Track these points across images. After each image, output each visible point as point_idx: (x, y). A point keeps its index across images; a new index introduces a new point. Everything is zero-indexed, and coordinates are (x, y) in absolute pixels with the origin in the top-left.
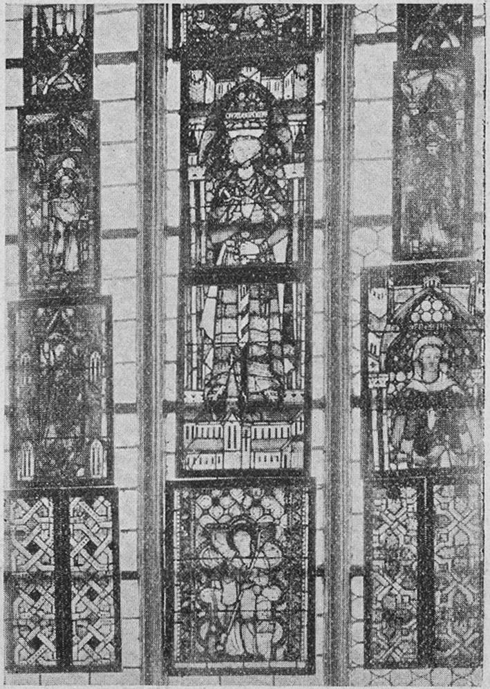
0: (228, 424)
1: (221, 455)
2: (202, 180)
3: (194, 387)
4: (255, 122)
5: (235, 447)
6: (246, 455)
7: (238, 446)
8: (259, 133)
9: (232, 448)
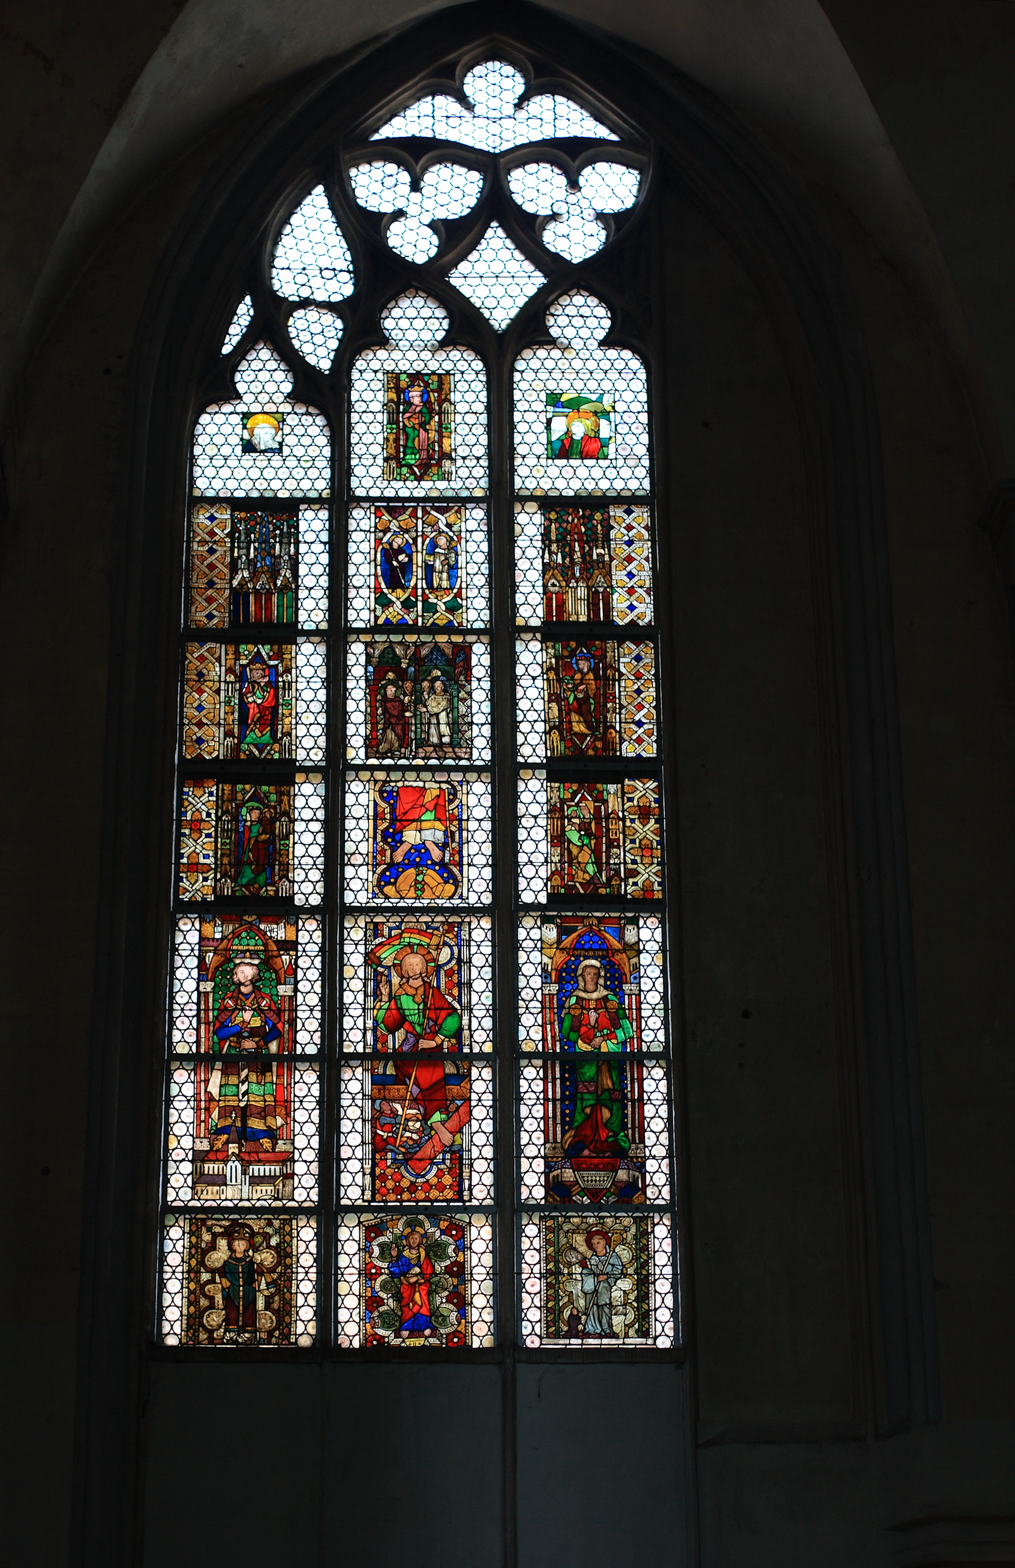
0: (230, 1163)
3: (202, 1135)
6: (246, 1188)
7: (239, 1181)
8: (256, 962)
9: (234, 1182)
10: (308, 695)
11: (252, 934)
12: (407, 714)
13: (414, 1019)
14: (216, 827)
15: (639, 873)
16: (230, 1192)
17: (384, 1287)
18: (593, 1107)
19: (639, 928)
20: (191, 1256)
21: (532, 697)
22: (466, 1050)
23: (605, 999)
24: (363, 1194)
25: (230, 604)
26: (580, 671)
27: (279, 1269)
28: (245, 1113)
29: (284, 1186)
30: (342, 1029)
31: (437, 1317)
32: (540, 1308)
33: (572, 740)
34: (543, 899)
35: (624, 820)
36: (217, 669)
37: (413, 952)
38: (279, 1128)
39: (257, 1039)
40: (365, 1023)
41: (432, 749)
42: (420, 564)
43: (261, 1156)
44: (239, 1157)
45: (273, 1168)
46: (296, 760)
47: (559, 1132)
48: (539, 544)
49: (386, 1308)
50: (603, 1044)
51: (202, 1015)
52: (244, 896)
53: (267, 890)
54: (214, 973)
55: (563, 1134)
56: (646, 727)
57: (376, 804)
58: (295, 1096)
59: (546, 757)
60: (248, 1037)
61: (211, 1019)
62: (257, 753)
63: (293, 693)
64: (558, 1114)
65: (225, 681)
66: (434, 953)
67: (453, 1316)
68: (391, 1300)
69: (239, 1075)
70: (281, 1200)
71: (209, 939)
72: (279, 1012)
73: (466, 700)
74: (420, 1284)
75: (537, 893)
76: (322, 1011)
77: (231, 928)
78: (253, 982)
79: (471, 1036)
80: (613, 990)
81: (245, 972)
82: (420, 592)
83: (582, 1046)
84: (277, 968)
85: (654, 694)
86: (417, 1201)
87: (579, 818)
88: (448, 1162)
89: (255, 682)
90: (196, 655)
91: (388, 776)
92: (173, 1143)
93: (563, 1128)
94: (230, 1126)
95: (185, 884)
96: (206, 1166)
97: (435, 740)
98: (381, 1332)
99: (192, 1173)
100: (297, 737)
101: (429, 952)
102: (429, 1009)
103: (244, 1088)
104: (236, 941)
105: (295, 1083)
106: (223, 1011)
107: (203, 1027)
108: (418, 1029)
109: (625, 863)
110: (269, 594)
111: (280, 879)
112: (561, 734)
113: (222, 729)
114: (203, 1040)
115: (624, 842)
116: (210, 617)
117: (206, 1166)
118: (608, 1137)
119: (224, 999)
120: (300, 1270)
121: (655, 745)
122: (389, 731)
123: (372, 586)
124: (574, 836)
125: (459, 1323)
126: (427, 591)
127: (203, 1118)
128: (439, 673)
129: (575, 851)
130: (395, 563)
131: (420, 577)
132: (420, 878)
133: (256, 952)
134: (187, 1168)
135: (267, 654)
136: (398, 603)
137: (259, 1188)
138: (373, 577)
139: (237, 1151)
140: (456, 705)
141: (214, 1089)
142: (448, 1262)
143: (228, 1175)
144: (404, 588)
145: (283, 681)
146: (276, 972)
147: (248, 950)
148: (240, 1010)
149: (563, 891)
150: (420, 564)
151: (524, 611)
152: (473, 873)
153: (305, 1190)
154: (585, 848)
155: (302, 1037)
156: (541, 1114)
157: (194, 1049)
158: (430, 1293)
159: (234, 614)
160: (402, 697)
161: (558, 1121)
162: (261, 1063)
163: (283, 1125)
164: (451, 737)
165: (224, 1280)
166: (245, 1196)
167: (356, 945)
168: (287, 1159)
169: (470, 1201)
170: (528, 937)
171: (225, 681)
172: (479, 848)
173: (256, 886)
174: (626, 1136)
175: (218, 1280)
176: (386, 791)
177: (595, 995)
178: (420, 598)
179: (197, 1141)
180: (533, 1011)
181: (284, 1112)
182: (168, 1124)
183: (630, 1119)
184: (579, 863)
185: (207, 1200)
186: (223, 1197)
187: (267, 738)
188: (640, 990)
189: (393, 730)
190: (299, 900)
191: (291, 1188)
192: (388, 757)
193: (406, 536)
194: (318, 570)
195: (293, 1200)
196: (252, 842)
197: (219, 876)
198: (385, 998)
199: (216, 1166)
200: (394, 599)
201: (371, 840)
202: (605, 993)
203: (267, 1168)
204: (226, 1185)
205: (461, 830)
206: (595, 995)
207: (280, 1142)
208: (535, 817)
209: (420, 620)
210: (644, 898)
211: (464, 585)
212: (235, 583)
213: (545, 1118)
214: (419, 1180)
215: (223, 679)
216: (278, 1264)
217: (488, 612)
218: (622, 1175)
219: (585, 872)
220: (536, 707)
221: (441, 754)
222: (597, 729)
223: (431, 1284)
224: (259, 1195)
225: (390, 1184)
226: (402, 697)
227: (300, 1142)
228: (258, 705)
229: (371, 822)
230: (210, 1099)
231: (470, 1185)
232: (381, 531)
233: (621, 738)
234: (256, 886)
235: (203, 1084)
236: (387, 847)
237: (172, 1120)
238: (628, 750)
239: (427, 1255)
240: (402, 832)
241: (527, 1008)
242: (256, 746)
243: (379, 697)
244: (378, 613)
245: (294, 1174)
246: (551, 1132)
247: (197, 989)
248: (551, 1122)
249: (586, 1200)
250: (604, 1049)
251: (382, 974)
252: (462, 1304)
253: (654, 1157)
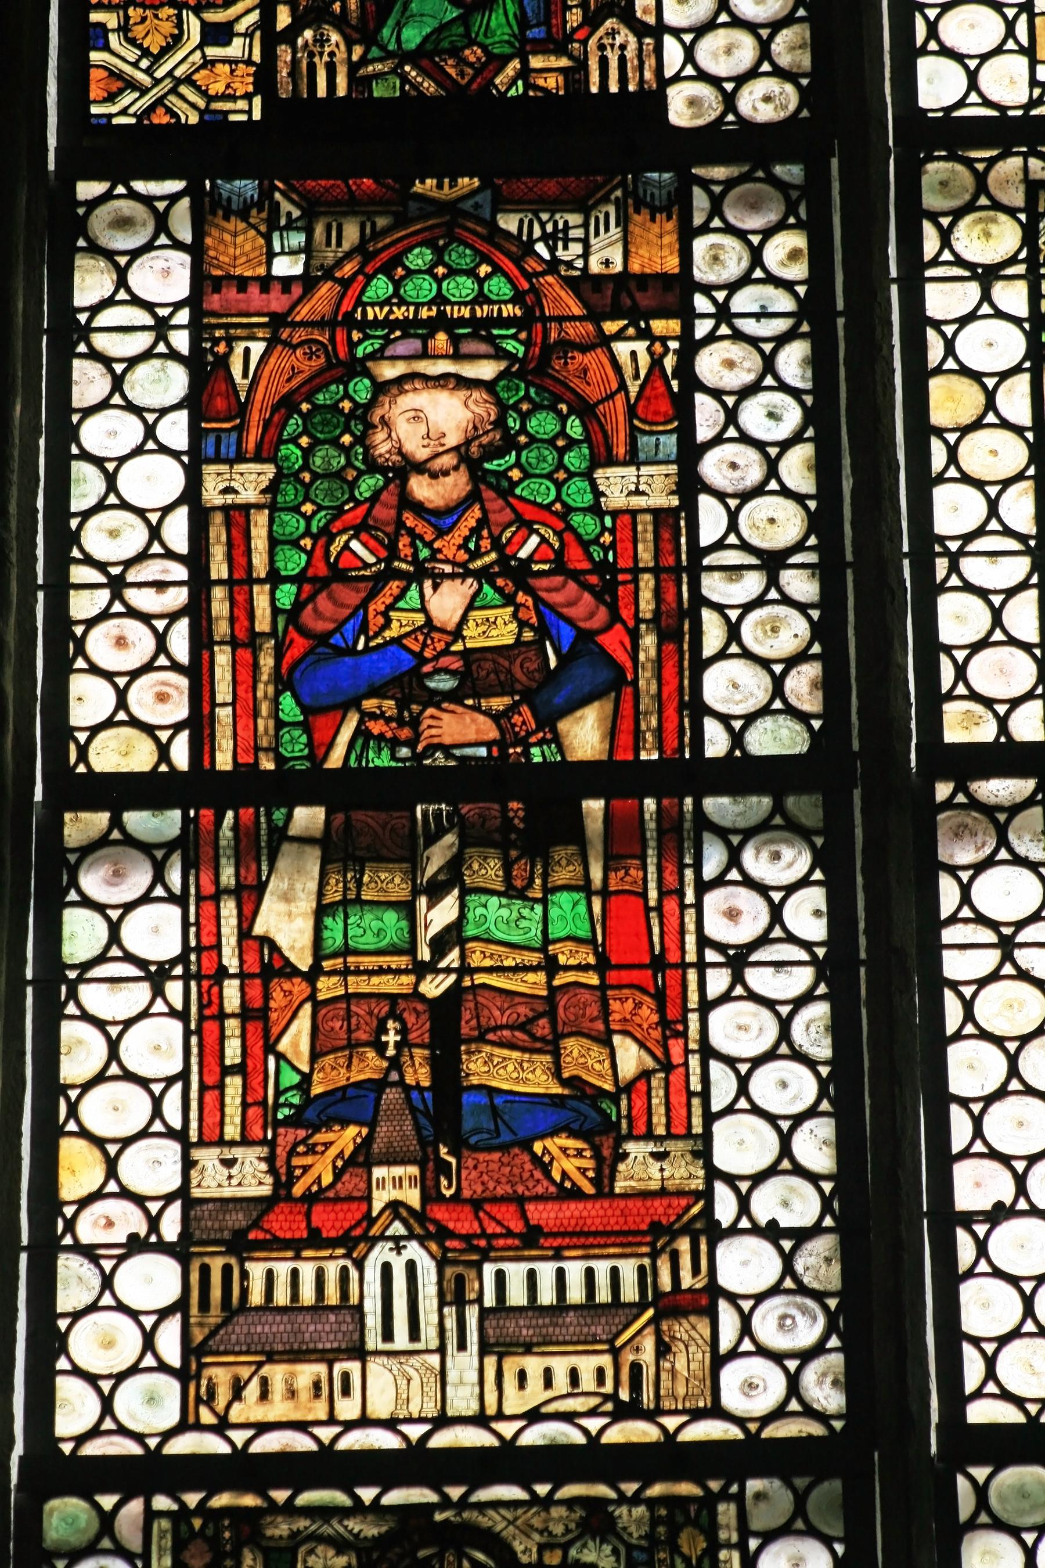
0: (381, 1253)
1: (354, 1367)
2: (259, 507)
3: (232, 1131)
4: (474, 336)
5: (414, 1333)
6: (464, 1365)
7: (429, 1335)
8: (487, 370)
9: (401, 1340)
11: (460, 256)
16: (382, 1388)
28: (447, 1026)
29: (663, 1350)
30: (931, 647)
38: (629, 1088)
39: (498, 703)
43: (537, 1213)
44: (423, 1225)
45: (602, 1268)
51: (219, 603)
52: (411, 102)
53: (525, 72)
58: (704, 942)
60: (455, 696)
61: (262, 624)
69: (413, 863)
70: (651, 1416)
71: (242, 283)
72: (608, 582)
76: (828, 572)
77: (351, 233)
78: (470, 456)
84: (593, 393)
92: (78, 1170)
94: (379, 1085)
95: (114, 55)
96: (257, 1270)
99: (181, 1306)
103: (441, 915)
104: (381, 287)
105: (703, 887)
106: (322, 584)
107: (223, 658)
111: (592, 22)
114: (224, 714)
117: (257, 1270)
119: (327, 534)
127: (233, 1052)
133: (481, 328)
137: (533, 1365)
139: (413, 1197)
141: (287, 920)
143: (373, 1307)
146: (585, 410)
148: (409, 579)
157: (180, 755)
162: (524, 814)
163: (646, 1075)
179: (208, 1158)
181: (648, 1014)
182: (50, 1086)
185: (263, 1428)
186: (348, 1409)
190: (684, 107)
191: (700, 1357)
195: (717, 1411)
197: (284, 18)
199: (307, 1271)
204: (360, 1353)
224: (535, 1394)
227: (741, 1145)
230: (268, 965)
235: (229, 909)
237: (74, 1068)
245: (714, 1291)
247: (191, 495)
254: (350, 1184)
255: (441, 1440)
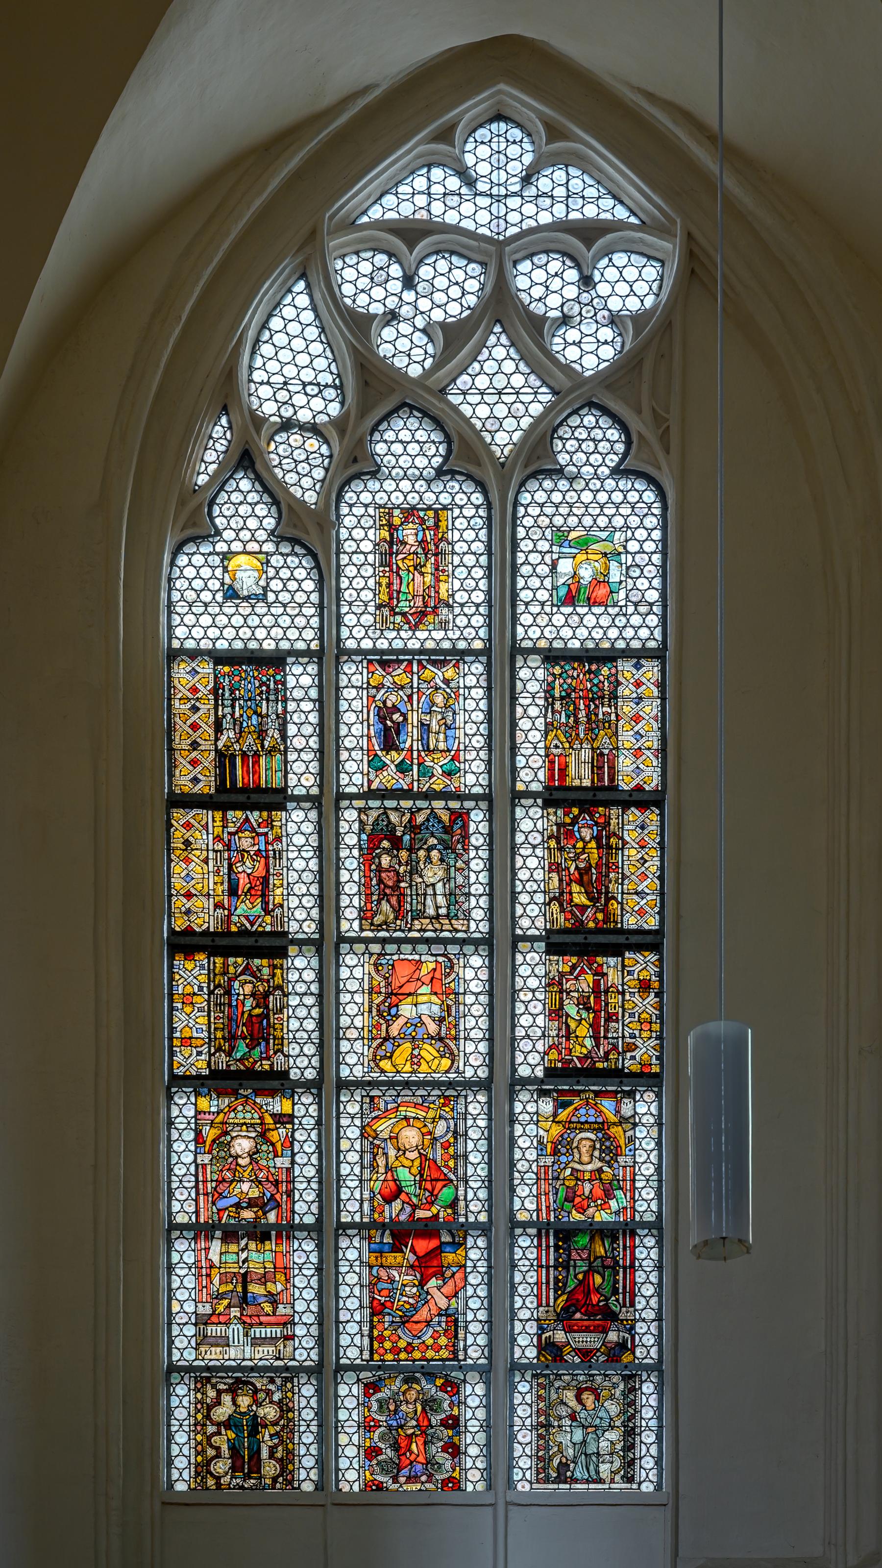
0: (232, 1326)
6: (248, 1349)
10: (299, 864)
12: (403, 885)
13: (411, 1190)
14: (209, 1001)
15: (637, 1047)
16: (233, 1353)
17: (382, 1438)
18: (585, 1273)
19: (635, 1102)
20: (198, 1411)
21: (531, 866)
22: (462, 1220)
23: (600, 1170)
24: (361, 1354)
25: (216, 767)
26: (582, 839)
27: (282, 1422)
31: (433, 1465)
32: (531, 1457)
33: (571, 912)
34: (539, 1072)
35: (623, 993)
36: (205, 837)
37: (409, 1125)
40: (362, 1194)
41: (428, 921)
42: (415, 724)
43: (263, 1319)
46: (288, 933)
47: (552, 1297)
48: (541, 702)
49: (384, 1456)
50: (597, 1214)
51: (201, 1186)
54: (211, 1146)
55: (556, 1300)
56: (649, 898)
57: (371, 978)
59: (545, 929)
60: (247, 1208)
62: (248, 925)
63: (284, 862)
64: (552, 1280)
65: (214, 850)
66: (430, 1126)
67: (448, 1465)
68: (389, 1450)
73: (463, 870)
74: (416, 1436)
75: (533, 1067)
79: (467, 1206)
80: (608, 1162)
81: (243, 1145)
82: (415, 754)
83: (576, 1216)
85: (658, 863)
86: (414, 1361)
87: (578, 991)
88: (443, 1325)
89: (244, 850)
90: (182, 822)
91: (383, 949)
93: (556, 1292)
94: (232, 1291)
97: (431, 911)
98: (380, 1478)
100: (289, 909)
101: (425, 1126)
102: (426, 1180)
108: (415, 1200)
109: (623, 1037)
110: (257, 755)
112: (561, 905)
113: (211, 900)
115: (623, 1016)
116: (195, 780)
118: (599, 1301)
120: (302, 1423)
121: (657, 917)
122: (384, 902)
123: (365, 747)
124: (571, 1009)
125: (454, 1470)
126: (423, 754)
127: (204, 1284)
128: (436, 842)
129: (573, 1025)
130: (388, 723)
131: (415, 738)
132: (416, 1052)
134: (190, 1331)
135: (256, 821)
136: (393, 767)
137: (261, 1349)
138: (365, 738)
140: (452, 875)
142: (443, 1416)
144: (398, 749)
145: (274, 850)
147: (245, 1124)
149: (560, 1065)
150: (415, 724)
151: (525, 775)
152: (470, 1047)
153: (305, 1351)
154: (583, 1022)
155: (300, 1207)
156: (533, 1280)
158: (425, 1443)
159: (221, 777)
160: (397, 866)
161: (552, 1286)
164: (448, 908)
165: (229, 1432)
166: (247, 1356)
167: (353, 1118)
168: (289, 1322)
169: (465, 1360)
170: (524, 1111)
171: (214, 850)
172: (474, 1021)
173: (251, 1060)
174: (617, 1300)
175: (223, 1432)
176: (381, 964)
177: (589, 1167)
178: (416, 761)
180: (528, 1182)
183: (621, 1284)
184: (577, 1037)
186: (226, 1357)
187: (258, 910)
188: (635, 1162)
189: (388, 901)
192: (383, 930)
193: (401, 693)
194: (308, 730)
195: (294, 1359)
196: (246, 1016)
198: (382, 1170)
200: (388, 762)
201: (366, 1014)
202: (600, 1164)
203: (268, 1330)
205: (457, 1003)
206: (589, 1167)
207: (280, 1306)
208: (533, 991)
209: (415, 784)
210: (642, 1072)
211: (462, 747)
212: (220, 744)
213: (538, 1283)
214: (416, 1342)
215: (211, 847)
216: (281, 1417)
217: (486, 776)
218: (613, 1336)
219: (583, 1046)
220: (536, 877)
221: (438, 926)
222: (598, 900)
223: (427, 1435)
225: (388, 1345)
226: (397, 866)
228: (249, 875)
229: (366, 996)
231: (465, 1345)
232: (374, 687)
233: (622, 909)
234: (251, 1060)
236: (382, 1021)
238: (631, 922)
239: (423, 1409)
240: (397, 1006)
241: (522, 1179)
242: (247, 917)
243: (374, 867)
244: (372, 777)
246: (544, 1296)
247: (195, 1161)
248: (544, 1287)
249: (577, 1360)
250: (597, 1218)
251: (378, 1147)
252: (455, 1450)
253: (644, 1320)
254: (227, 1312)
255: (244, 1363)
